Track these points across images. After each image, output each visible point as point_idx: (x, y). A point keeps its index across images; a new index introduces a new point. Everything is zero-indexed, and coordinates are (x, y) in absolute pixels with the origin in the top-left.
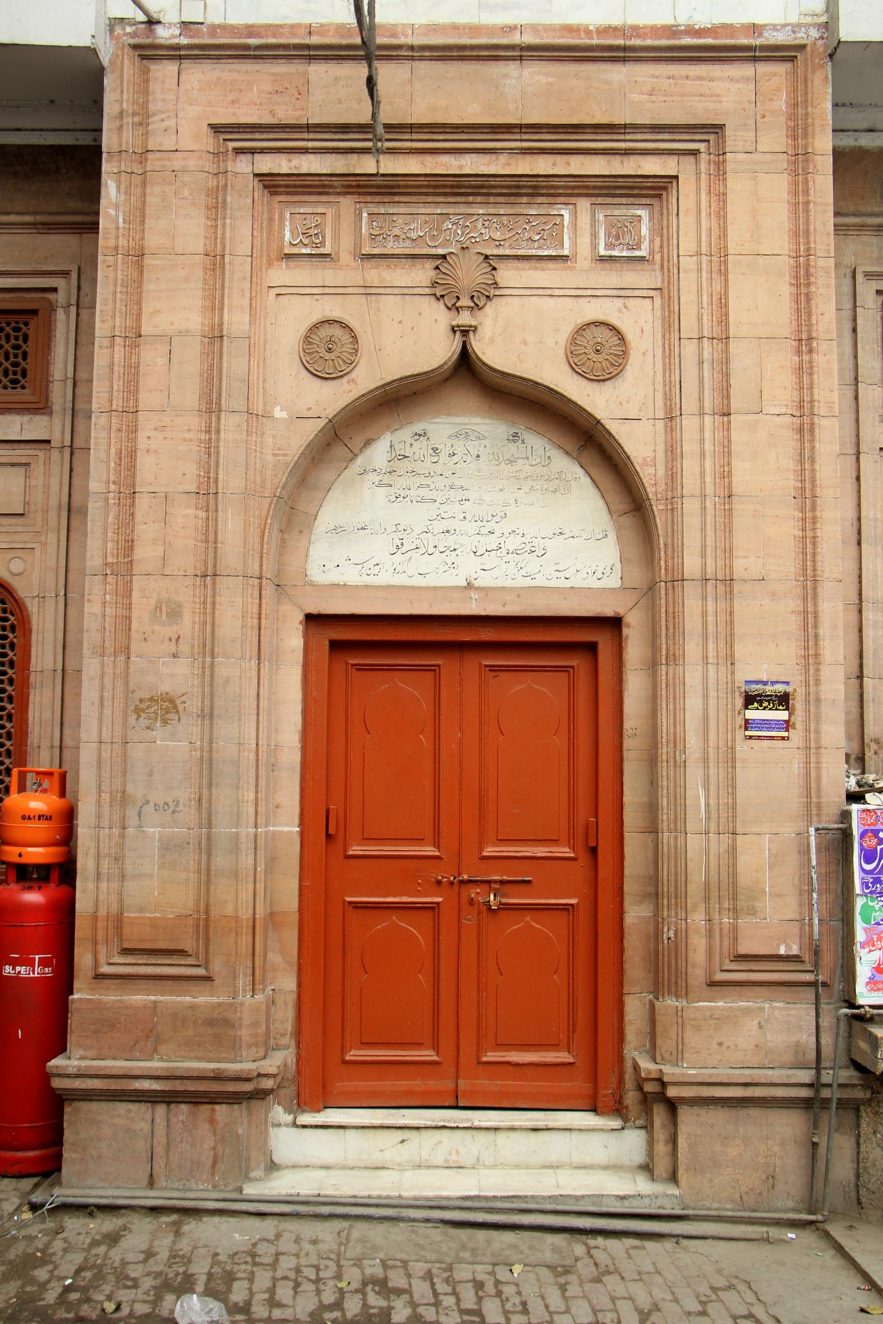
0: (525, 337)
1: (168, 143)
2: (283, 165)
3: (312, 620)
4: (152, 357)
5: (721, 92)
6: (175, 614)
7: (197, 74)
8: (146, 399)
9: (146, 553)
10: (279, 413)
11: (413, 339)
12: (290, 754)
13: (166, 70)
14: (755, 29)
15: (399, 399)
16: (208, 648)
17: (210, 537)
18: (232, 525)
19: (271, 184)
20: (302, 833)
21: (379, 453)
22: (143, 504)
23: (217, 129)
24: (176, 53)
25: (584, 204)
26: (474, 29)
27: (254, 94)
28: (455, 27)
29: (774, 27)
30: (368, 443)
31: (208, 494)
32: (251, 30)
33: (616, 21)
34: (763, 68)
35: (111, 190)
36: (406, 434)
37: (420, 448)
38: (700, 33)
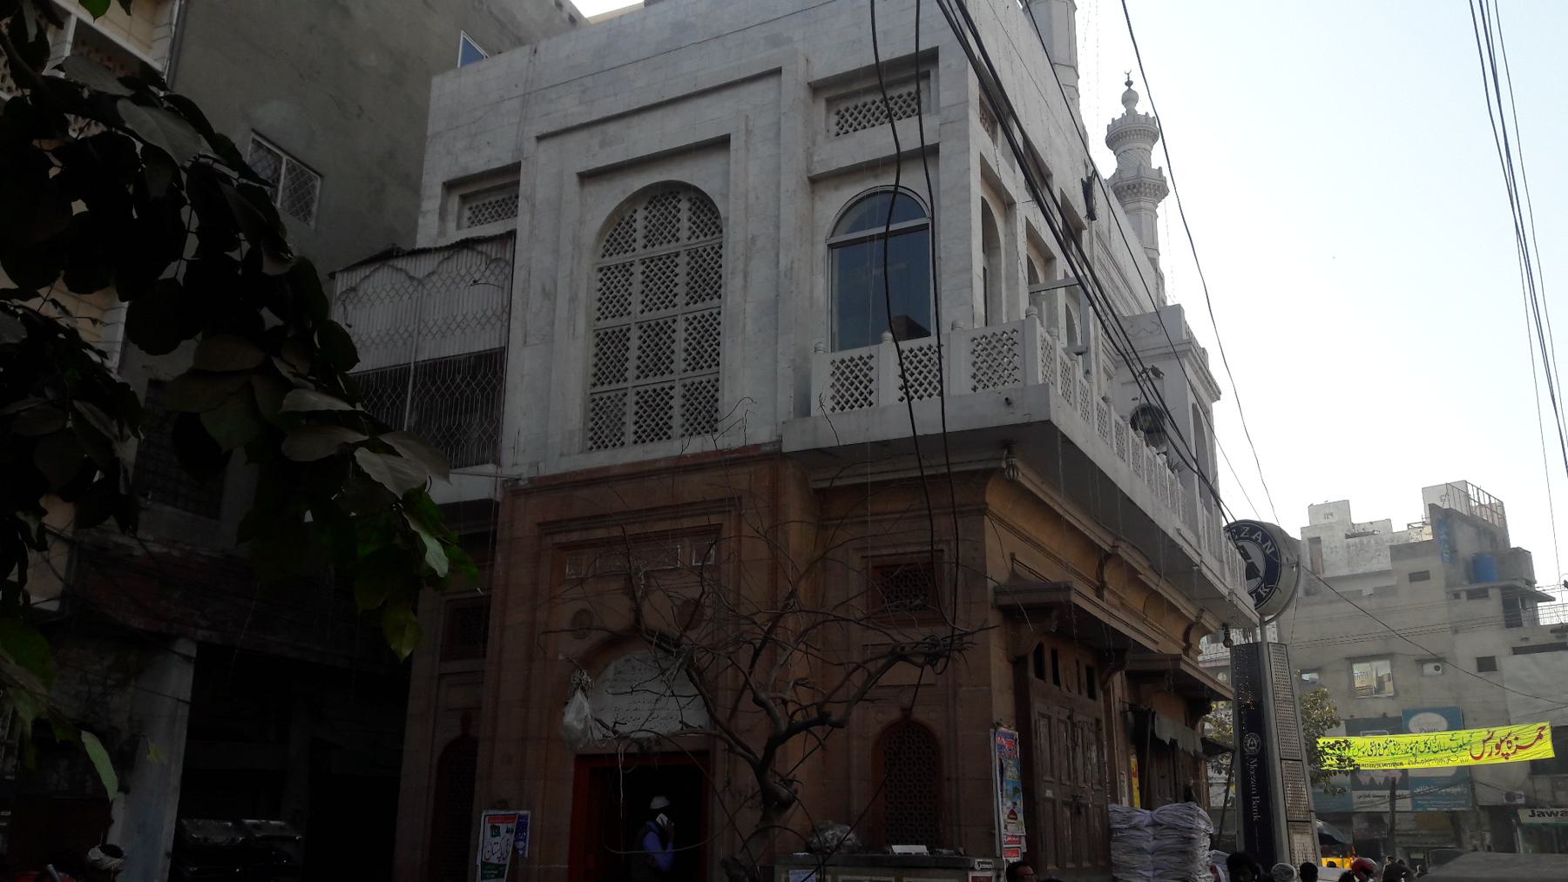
0: (659, 614)
2: (562, 538)
3: (582, 760)
10: (561, 657)
11: (616, 614)
14: (757, 446)
15: (615, 643)
21: (610, 672)
23: (539, 524)
24: (526, 492)
25: (687, 541)
29: (765, 444)
30: (606, 666)
32: (555, 477)
33: (698, 451)
35: (499, 558)
38: (737, 451)
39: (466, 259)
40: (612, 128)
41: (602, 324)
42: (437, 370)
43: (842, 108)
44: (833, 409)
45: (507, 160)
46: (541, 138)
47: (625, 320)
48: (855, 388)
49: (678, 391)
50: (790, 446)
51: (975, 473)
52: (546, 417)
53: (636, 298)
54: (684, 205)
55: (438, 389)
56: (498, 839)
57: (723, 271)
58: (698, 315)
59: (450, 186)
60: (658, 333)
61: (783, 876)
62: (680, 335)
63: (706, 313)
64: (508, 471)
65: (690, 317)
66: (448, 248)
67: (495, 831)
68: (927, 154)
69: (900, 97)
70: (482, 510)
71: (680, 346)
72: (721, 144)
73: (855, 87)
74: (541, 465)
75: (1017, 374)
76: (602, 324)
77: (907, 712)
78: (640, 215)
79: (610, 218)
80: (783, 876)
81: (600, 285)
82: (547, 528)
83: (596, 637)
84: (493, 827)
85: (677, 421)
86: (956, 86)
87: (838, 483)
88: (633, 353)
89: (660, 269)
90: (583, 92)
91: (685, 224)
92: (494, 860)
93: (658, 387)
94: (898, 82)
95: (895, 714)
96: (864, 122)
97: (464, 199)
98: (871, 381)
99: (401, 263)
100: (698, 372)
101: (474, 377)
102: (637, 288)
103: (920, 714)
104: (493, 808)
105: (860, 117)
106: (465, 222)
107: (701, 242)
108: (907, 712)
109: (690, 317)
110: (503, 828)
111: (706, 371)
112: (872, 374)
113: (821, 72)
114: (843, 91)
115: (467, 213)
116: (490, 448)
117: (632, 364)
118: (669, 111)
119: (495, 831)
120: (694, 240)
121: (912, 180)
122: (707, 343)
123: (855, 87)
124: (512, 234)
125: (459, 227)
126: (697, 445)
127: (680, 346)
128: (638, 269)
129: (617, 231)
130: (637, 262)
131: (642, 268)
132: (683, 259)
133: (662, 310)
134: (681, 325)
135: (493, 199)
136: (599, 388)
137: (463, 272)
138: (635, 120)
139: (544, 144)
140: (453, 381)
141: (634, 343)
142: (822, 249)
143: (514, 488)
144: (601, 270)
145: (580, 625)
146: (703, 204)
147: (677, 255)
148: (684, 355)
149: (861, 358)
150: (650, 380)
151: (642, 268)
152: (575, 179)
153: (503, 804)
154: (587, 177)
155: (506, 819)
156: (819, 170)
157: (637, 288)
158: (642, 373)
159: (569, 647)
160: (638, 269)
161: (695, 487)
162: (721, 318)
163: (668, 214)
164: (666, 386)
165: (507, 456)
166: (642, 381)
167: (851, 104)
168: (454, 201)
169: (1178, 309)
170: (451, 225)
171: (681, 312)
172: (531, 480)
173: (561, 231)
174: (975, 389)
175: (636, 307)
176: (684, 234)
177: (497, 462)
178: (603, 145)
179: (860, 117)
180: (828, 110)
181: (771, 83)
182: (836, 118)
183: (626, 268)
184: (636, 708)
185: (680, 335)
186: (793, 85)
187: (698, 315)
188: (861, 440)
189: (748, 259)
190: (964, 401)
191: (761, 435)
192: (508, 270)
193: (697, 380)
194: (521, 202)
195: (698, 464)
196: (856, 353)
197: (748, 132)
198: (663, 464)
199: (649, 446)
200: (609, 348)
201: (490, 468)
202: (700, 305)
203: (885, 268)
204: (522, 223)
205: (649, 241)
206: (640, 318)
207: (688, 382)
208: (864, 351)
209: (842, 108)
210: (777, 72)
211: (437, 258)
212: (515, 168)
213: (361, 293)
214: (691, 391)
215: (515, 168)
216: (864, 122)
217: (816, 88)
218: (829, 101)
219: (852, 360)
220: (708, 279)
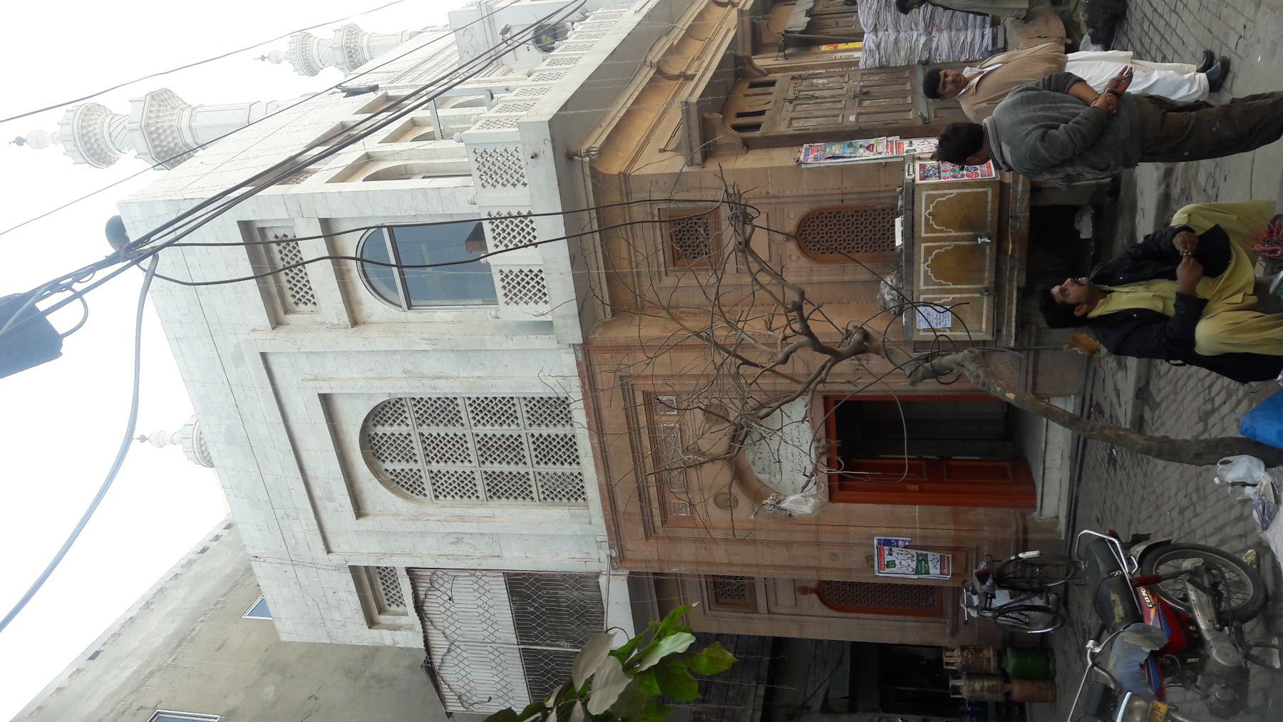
0: (716, 441)
1: (655, 555)
2: (658, 520)
3: (832, 499)
4: (736, 559)
5: (605, 379)
6: (834, 555)
7: (629, 545)
8: (752, 561)
9: (812, 563)
11: (718, 475)
12: (886, 508)
13: (628, 555)
15: (740, 475)
16: (847, 545)
17: (805, 543)
18: (799, 537)
19: (664, 522)
20: (919, 504)
22: (792, 563)
26: (595, 458)
27: (634, 529)
28: (596, 465)
31: (788, 544)
32: (608, 528)
34: (595, 362)
35: (674, 570)
36: (754, 468)
37: (759, 463)
39: (430, 608)
40: (317, 492)
41: (481, 494)
42: (525, 626)
43: (292, 300)
44: (546, 302)
45: (348, 577)
46: (329, 551)
47: (477, 476)
48: (528, 285)
49: (536, 430)
50: (579, 339)
51: (594, 185)
52: (562, 537)
53: (459, 467)
54: (380, 430)
55: (539, 625)
56: (897, 562)
57: (434, 397)
58: (471, 416)
59: (371, 623)
60: (488, 448)
61: (921, 333)
62: (489, 430)
63: (469, 409)
64: (604, 566)
65: (473, 422)
66: (422, 619)
67: (891, 564)
68: (329, 230)
69: (281, 252)
70: (635, 583)
71: (498, 430)
72: (326, 400)
73: (274, 290)
74: (599, 539)
75: (511, 149)
76: (481, 494)
77: (788, 236)
78: (388, 466)
79: (393, 491)
80: (921, 333)
81: (449, 497)
82: (650, 532)
83: (736, 490)
84: (888, 566)
85: (560, 430)
86: (269, 207)
87: (607, 297)
88: (505, 468)
89: (435, 449)
90: (288, 516)
91: (396, 429)
92: (914, 565)
93: (532, 447)
94: (268, 256)
95: (792, 246)
96: (304, 282)
97: (381, 611)
98: (521, 271)
99: (437, 660)
100: (518, 414)
101: (529, 597)
102: (451, 467)
103: (791, 226)
104: (873, 566)
105: (299, 285)
106: (401, 609)
107: (410, 414)
108: (788, 236)
109: (473, 422)
110: (888, 558)
111: (517, 408)
112: (516, 271)
113: (263, 320)
114: (278, 300)
115: (394, 607)
116: (586, 582)
117: (514, 468)
118: (300, 444)
119: (891, 564)
120: (409, 421)
121: (350, 245)
122: (494, 408)
123: (274, 290)
124: (410, 571)
125: (405, 614)
126: (579, 415)
127: (498, 430)
128: (435, 467)
129: (405, 485)
130: (430, 467)
131: (434, 463)
132: (425, 430)
133: (469, 445)
134: (481, 430)
135: (381, 587)
136: (535, 495)
137: (443, 609)
138: (310, 473)
139: (333, 547)
140: (532, 613)
141: (497, 467)
142: (412, 315)
143: (618, 560)
144: (436, 497)
145: (725, 502)
146: (378, 414)
147: (422, 435)
148: (505, 426)
149: (503, 280)
150: (526, 453)
151: (434, 463)
152: (361, 521)
153: (870, 558)
154: (359, 512)
155: (881, 555)
156: (345, 318)
157: (451, 467)
158: (521, 460)
159: (744, 510)
160: (435, 467)
161: (614, 415)
162: (473, 397)
163: (388, 443)
164: (531, 440)
165: (593, 567)
166: (528, 460)
167: (289, 293)
168: (383, 619)
169: (451, 15)
170: (403, 620)
171: (470, 430)
172: (611, 548)
173: (405, 531)
174: (525, 185)
175: (467, 467)
176: (404, 430)
177: (598, 575)
178: (332, 499)
179: (299, 285)
180: (295, 312)
181: (273, 360)
182: (301, 305)
183: (435, 476)
184: (793, 453)
185: (489, 430)
186: (276, 342)
187: (471, 416)
188: (569, 279)
189: (423, 377)
190: (536, 193)
191: (568, 363)
192: (439, 573)
193: (526, 415)
194: (382, 564)
195: (595, 413)
196: (498, 285)
197: (316, 379)
198: (596, 441)
199: (581, 452)
200: (500, 488)
201: (602, 581)
202: (463, 415)
203: (429, 262)
204: (400, 564)
205: (411, 458)
206: (475, 463)
207: (527, 422)
208: (497, 278)
209: (292, 300)
210: (264, 356)
211: (432, 632)
212: (354, 570)
213: (463, 691)
214: (534, 420)
215: (354, 570)
216: (304, 282)
217: (276, 323)
218: (286, 312)
219: (504, 287)
220: (440, 409)
